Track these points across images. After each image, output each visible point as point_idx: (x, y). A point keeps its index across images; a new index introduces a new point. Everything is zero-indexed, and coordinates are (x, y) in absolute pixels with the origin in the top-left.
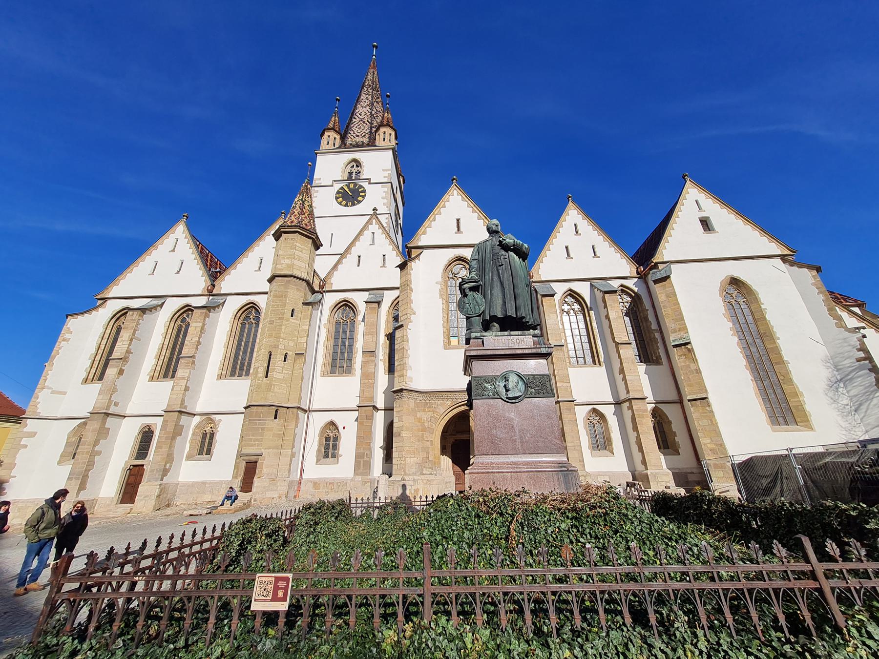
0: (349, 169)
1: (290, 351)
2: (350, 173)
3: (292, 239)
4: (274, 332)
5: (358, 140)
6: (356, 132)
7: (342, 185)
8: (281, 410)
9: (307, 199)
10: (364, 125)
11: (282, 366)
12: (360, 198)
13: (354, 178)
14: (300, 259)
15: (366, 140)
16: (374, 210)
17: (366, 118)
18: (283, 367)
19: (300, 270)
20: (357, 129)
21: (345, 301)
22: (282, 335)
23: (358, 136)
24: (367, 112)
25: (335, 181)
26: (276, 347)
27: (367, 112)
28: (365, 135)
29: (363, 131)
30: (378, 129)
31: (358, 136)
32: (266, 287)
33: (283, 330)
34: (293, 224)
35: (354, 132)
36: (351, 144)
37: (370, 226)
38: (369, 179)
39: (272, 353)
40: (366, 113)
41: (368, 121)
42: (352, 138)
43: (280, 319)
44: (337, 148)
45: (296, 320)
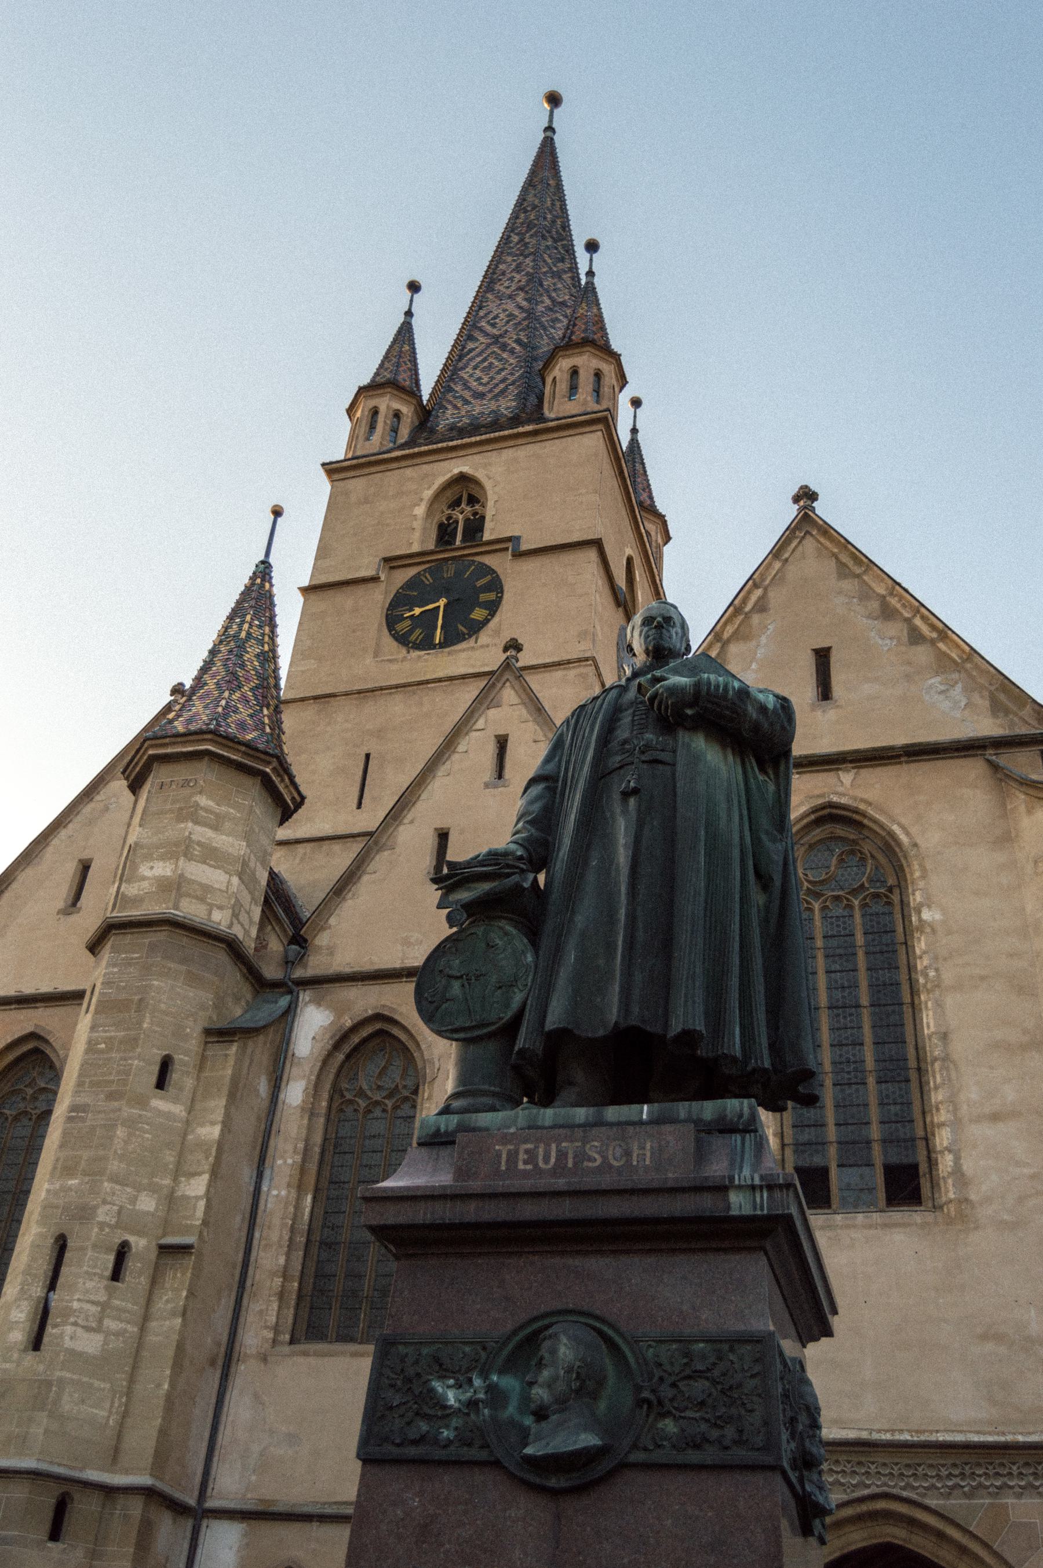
0: (440, 517)
1: (140, 1233)
2: (445, 533)
3: (185, 784)
4: (86, 1154)
7: (412, 572)
8: (84, 1507)
9: (256, 632)
11: (102, 1297)
12: (478, 614)
13: (458, 543)
14: (211, 856)
16: (506, 649)
18: (104, 1306)
19: (202, 900)
21: (378, 1017)
22: (115, 1166)
23: (481, 396)
24: (516, 312)
25: (386, 560)
26: (84, 1214)
27: (516, 312)
28: (506, 388)
29: (499, 377)
31: (481, 396)
33: (118, 1144)
34: (193, 727)
36: (452, 428)
37: (492, 713)
38: (514, 540)
39: (70, 1244)
40: (511, 316)
41: (518, 341)
43: (111, 1096)
44: (402, 447)
45: (176, 1100)
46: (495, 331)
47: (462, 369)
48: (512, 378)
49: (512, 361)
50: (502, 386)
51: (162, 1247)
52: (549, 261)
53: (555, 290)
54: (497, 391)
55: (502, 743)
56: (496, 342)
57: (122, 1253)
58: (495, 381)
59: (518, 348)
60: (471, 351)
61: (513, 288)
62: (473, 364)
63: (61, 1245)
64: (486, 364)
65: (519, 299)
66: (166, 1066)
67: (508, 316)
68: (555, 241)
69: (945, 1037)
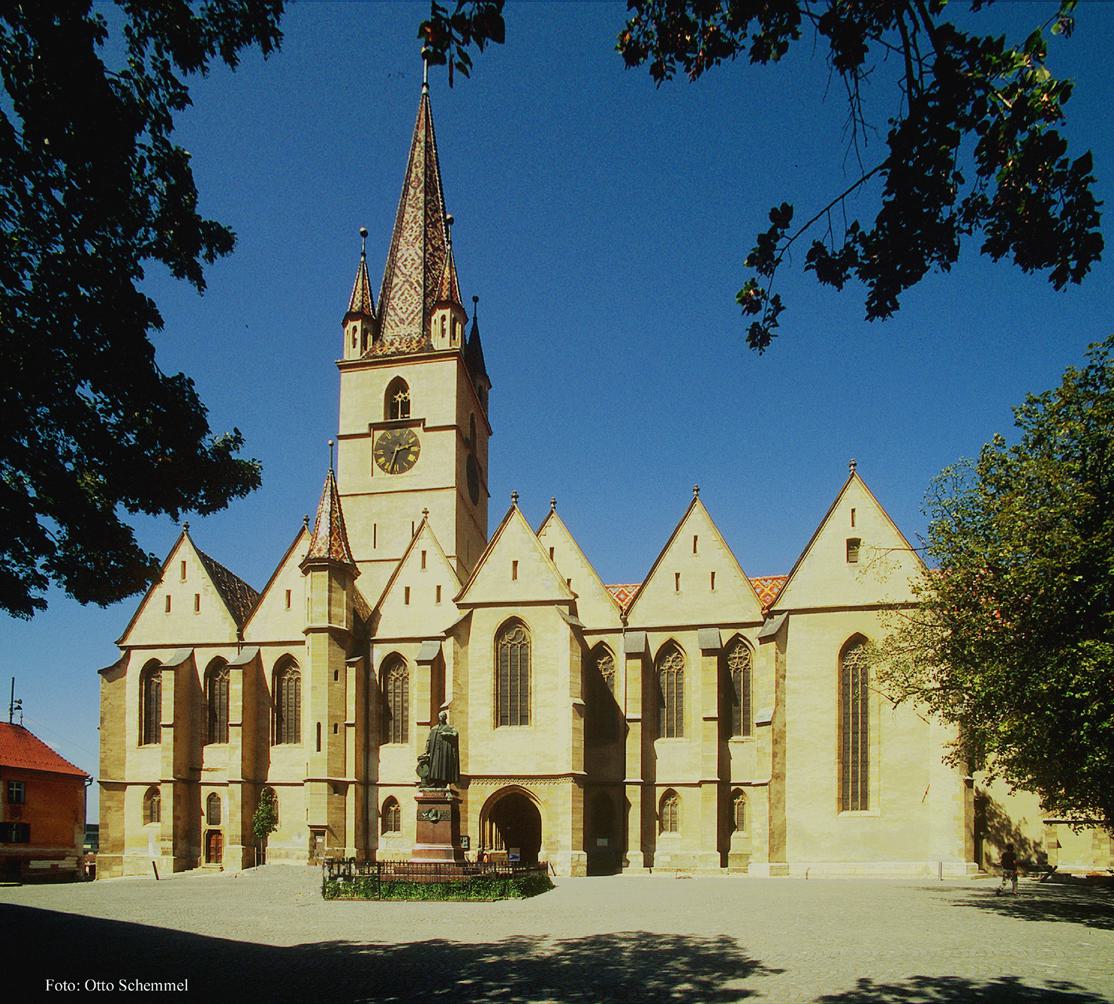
5: (404, 330)
6: (399, 312)
10: (412, 292)
15: (416, 330)
17: (414, 276)
20: (401, 305)
23: (402, 321)
28: (414, 319)
29: (410, 309)
30: (432, 312)
31: (402, 321)
32: (302, 637)
35: (394, 309)
37: (420, 541)
41: (417, 281)
42: (392, 323)
46: (405, 271)
47: (393, 299)
48: (417, 311)
49: (416, 297)
50: (412, 316)
51: (346, 725)
52: (430, 213)
53: (434, 238)
54: (410, 319)
55: (424, 553)
56: (407, 281)
57: (336, 726)
58: (409, 312)
59: (418, 289)
60: (396, 285)
61: (413, 237)
62: (397, 296)
63: (319, 725)
64: (403, 297)
65: (416, 247)
66: (336, 673)
67: (413, 260)
68: (432, 196)
69: (536, 686)
